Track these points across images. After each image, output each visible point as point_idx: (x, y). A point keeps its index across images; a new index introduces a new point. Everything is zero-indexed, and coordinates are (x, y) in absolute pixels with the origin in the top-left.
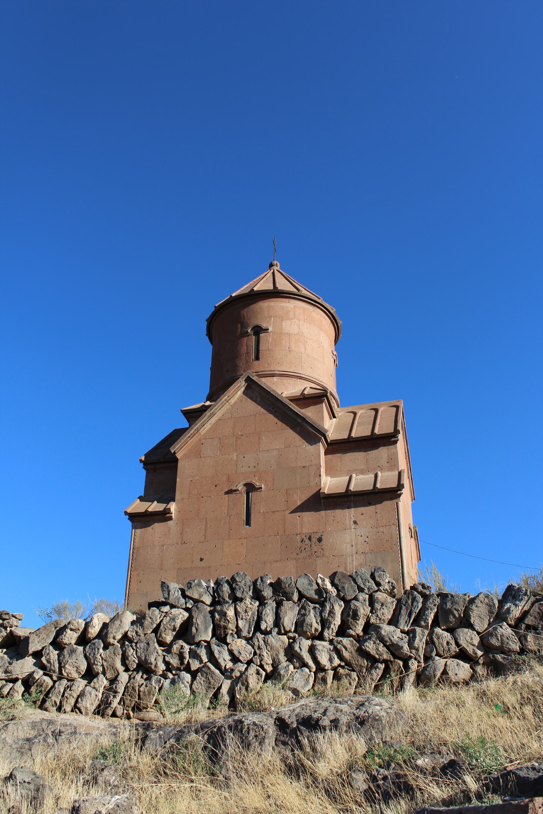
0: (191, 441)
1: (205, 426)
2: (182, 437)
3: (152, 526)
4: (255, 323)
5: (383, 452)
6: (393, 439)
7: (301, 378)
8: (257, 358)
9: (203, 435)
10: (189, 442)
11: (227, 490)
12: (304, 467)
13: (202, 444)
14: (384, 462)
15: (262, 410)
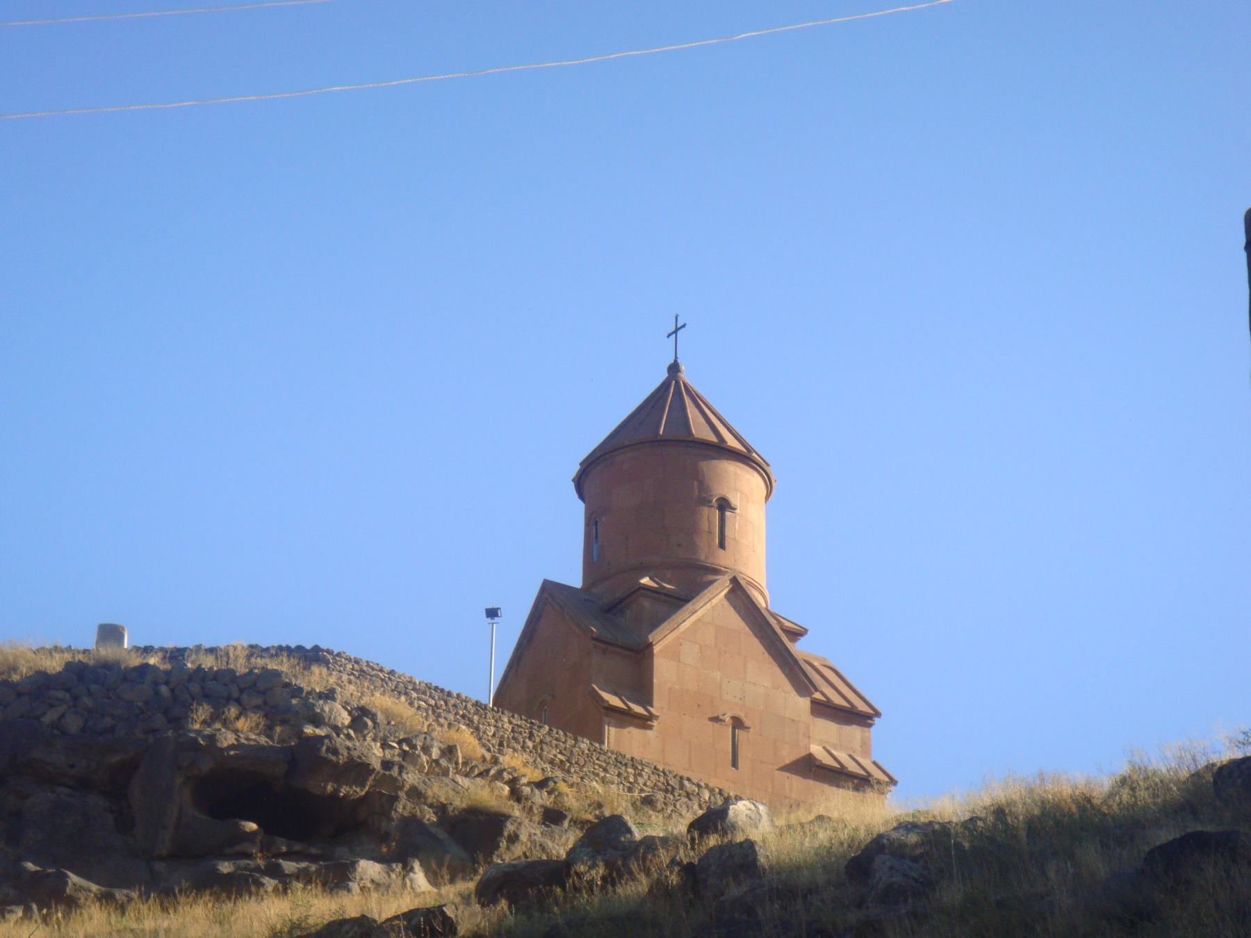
0: (669, 635)
1: (686, 623)
2: (663, 626)
3: (628, 729)
4: (721, 493)
5: (855, 731)
6: (869, 721)
7: (762, 594)
8: (722, 545)
9: (683, 633)
10: (668, 637)
11: (710, 716)
12: (793, 720)
13: (681, 645)
14: (857, 744)
15: (747, 628)
